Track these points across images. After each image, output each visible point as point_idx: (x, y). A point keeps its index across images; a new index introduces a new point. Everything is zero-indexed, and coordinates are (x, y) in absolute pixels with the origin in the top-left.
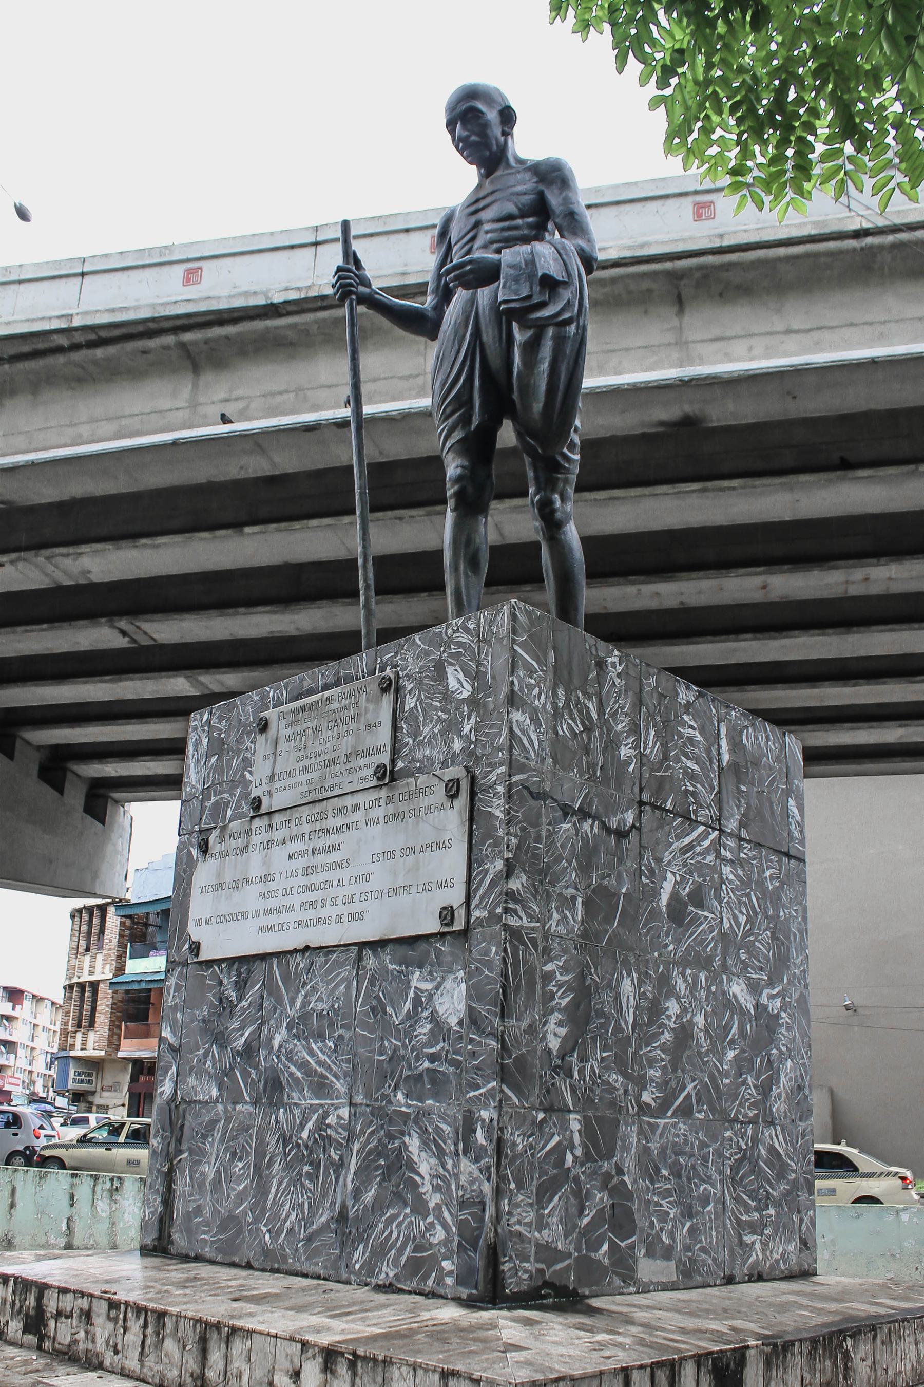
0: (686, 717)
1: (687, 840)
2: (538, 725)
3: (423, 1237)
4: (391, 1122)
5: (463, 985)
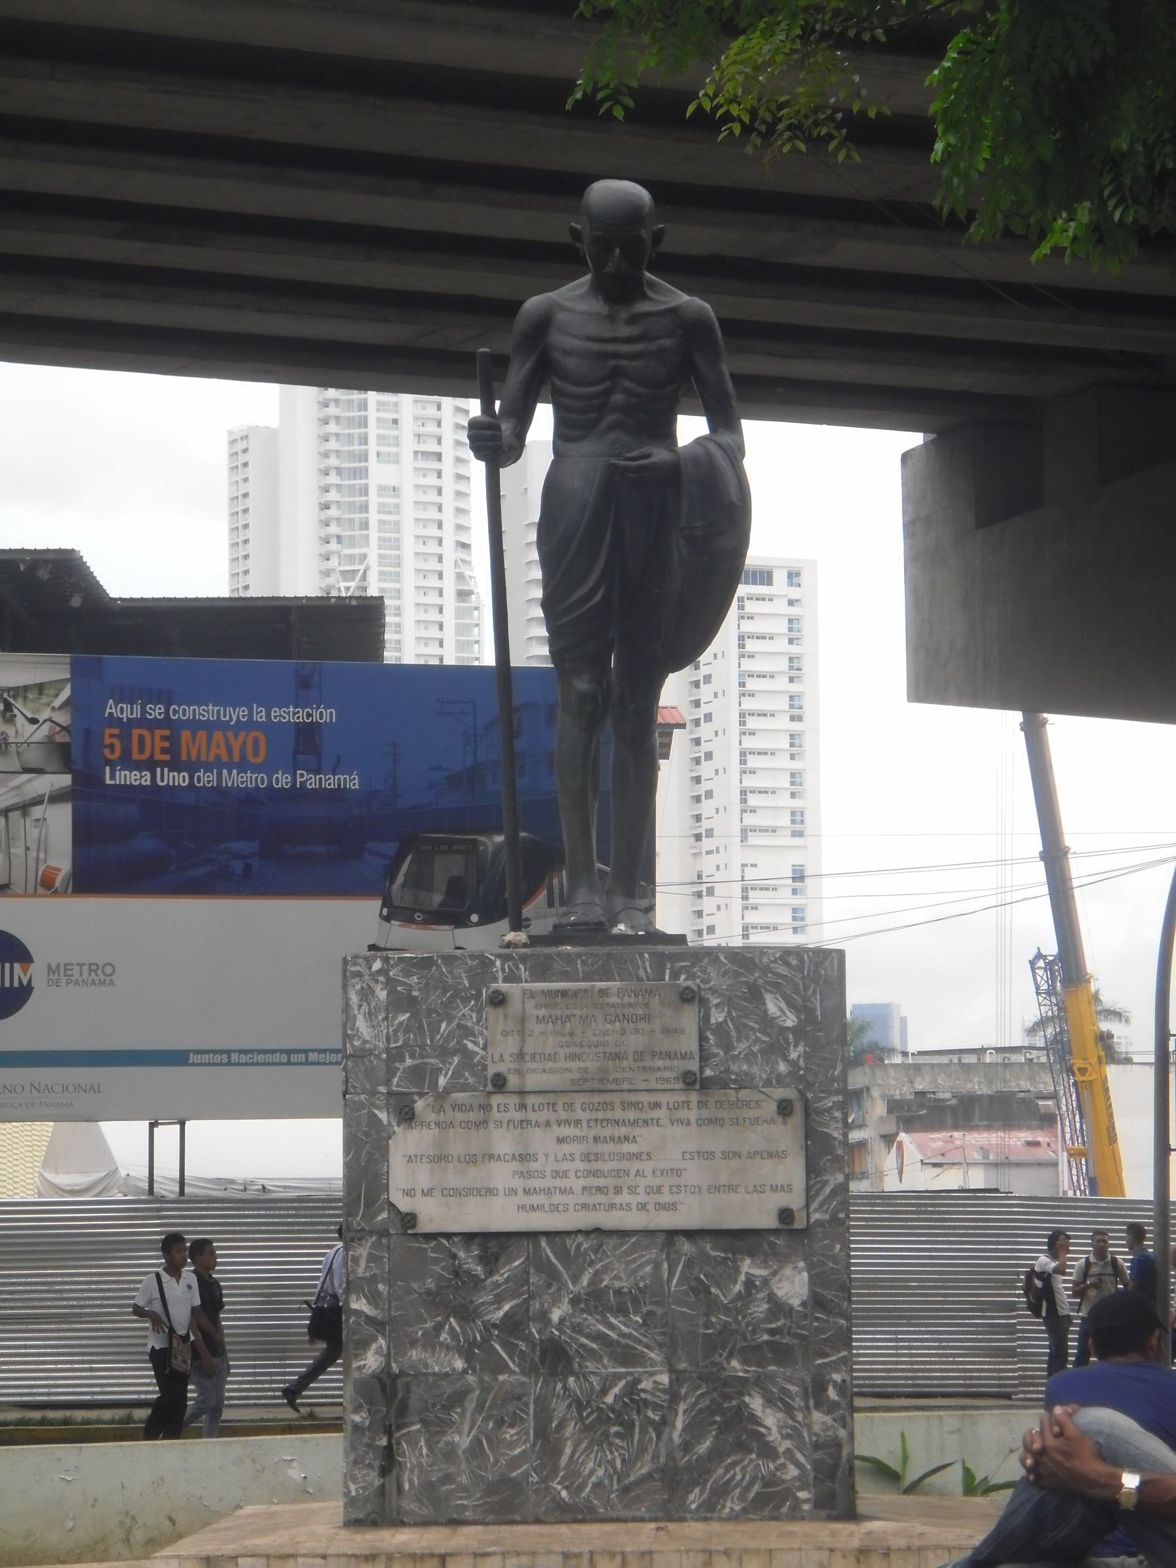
3: (774, 1475)
4: (725, 1384)
5: (805, 1275)
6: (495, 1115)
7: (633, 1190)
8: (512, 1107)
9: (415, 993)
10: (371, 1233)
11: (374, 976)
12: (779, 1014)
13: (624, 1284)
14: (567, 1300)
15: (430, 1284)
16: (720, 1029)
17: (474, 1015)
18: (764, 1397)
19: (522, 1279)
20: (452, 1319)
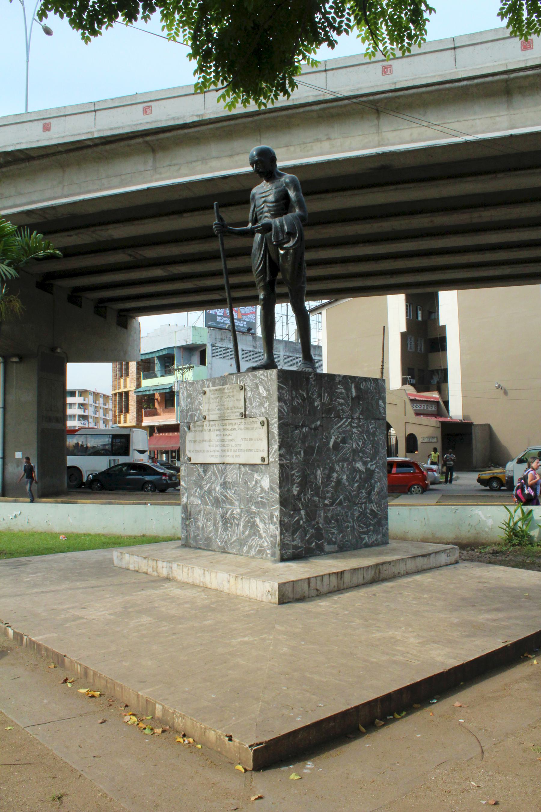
0: (339, 386)
1: (339, 425)
2: (286, 404)
4: (251, 514)
6: (205, 428)
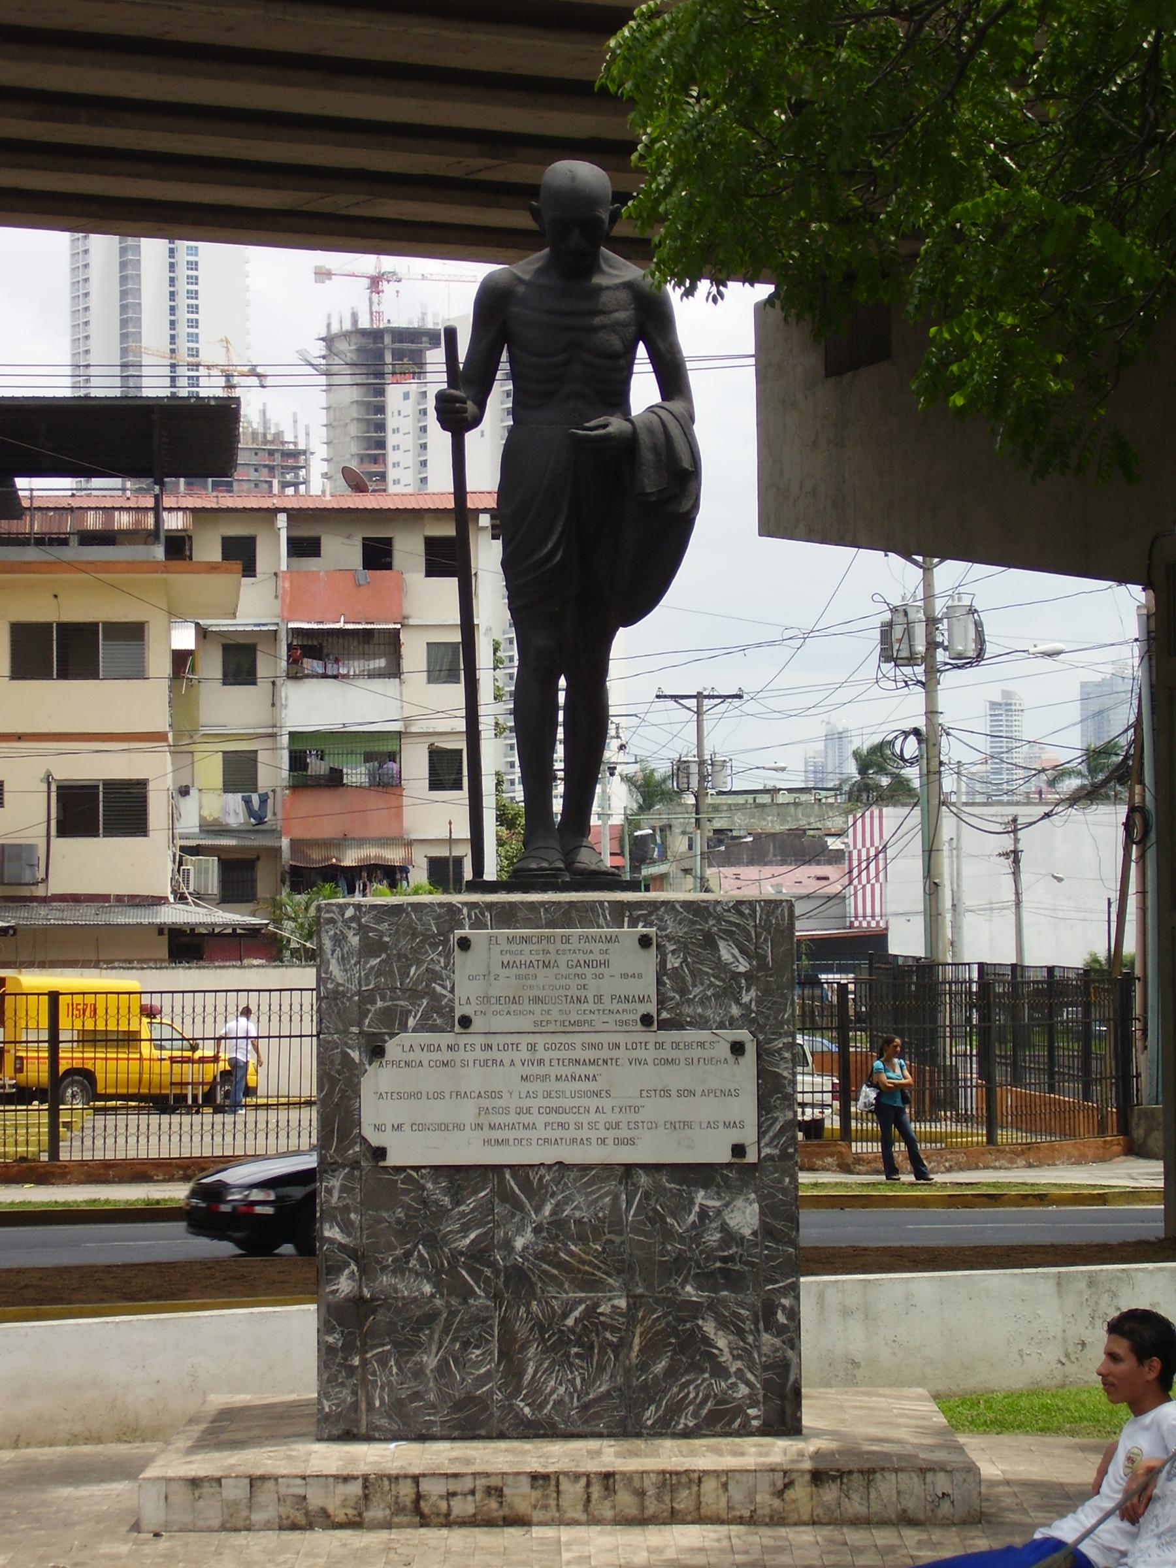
4: (680, 1309)
5: (756, 1206)
7: (592, 1126)
8: (478, 1048)
9: (387, 939)
10: (344, 1166)
11: (347, 922)
12: (732, 960)
13: (584, 1215)
14: (530, 1229)
15: (400, 1213)
16: (676, 973)
17: (442, 960)
18: (716, 1320)
19: (486, 1209)
20: (420, 1247)
